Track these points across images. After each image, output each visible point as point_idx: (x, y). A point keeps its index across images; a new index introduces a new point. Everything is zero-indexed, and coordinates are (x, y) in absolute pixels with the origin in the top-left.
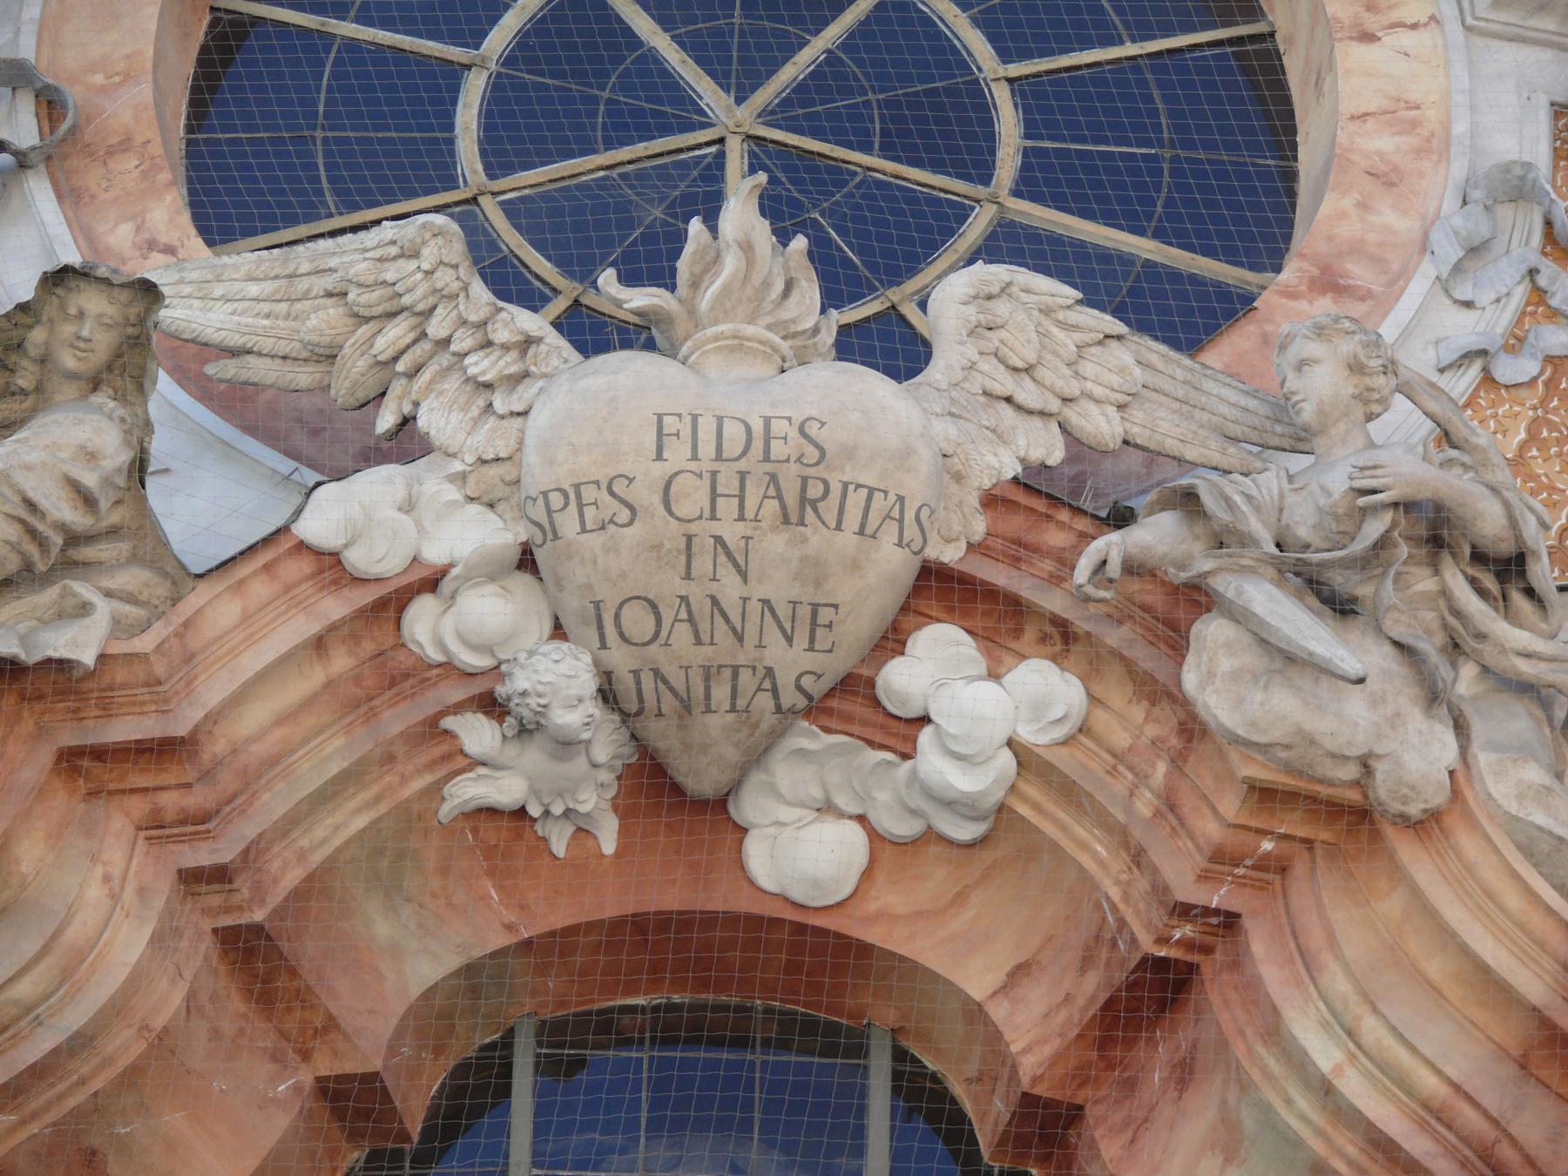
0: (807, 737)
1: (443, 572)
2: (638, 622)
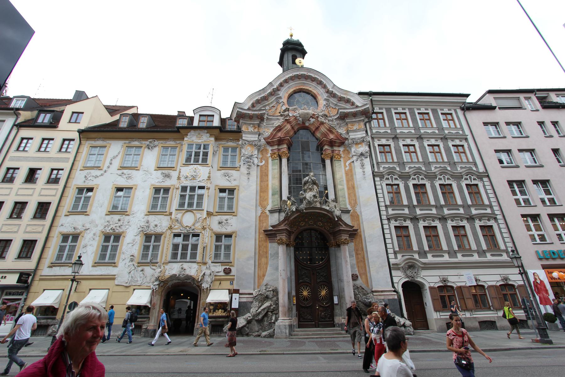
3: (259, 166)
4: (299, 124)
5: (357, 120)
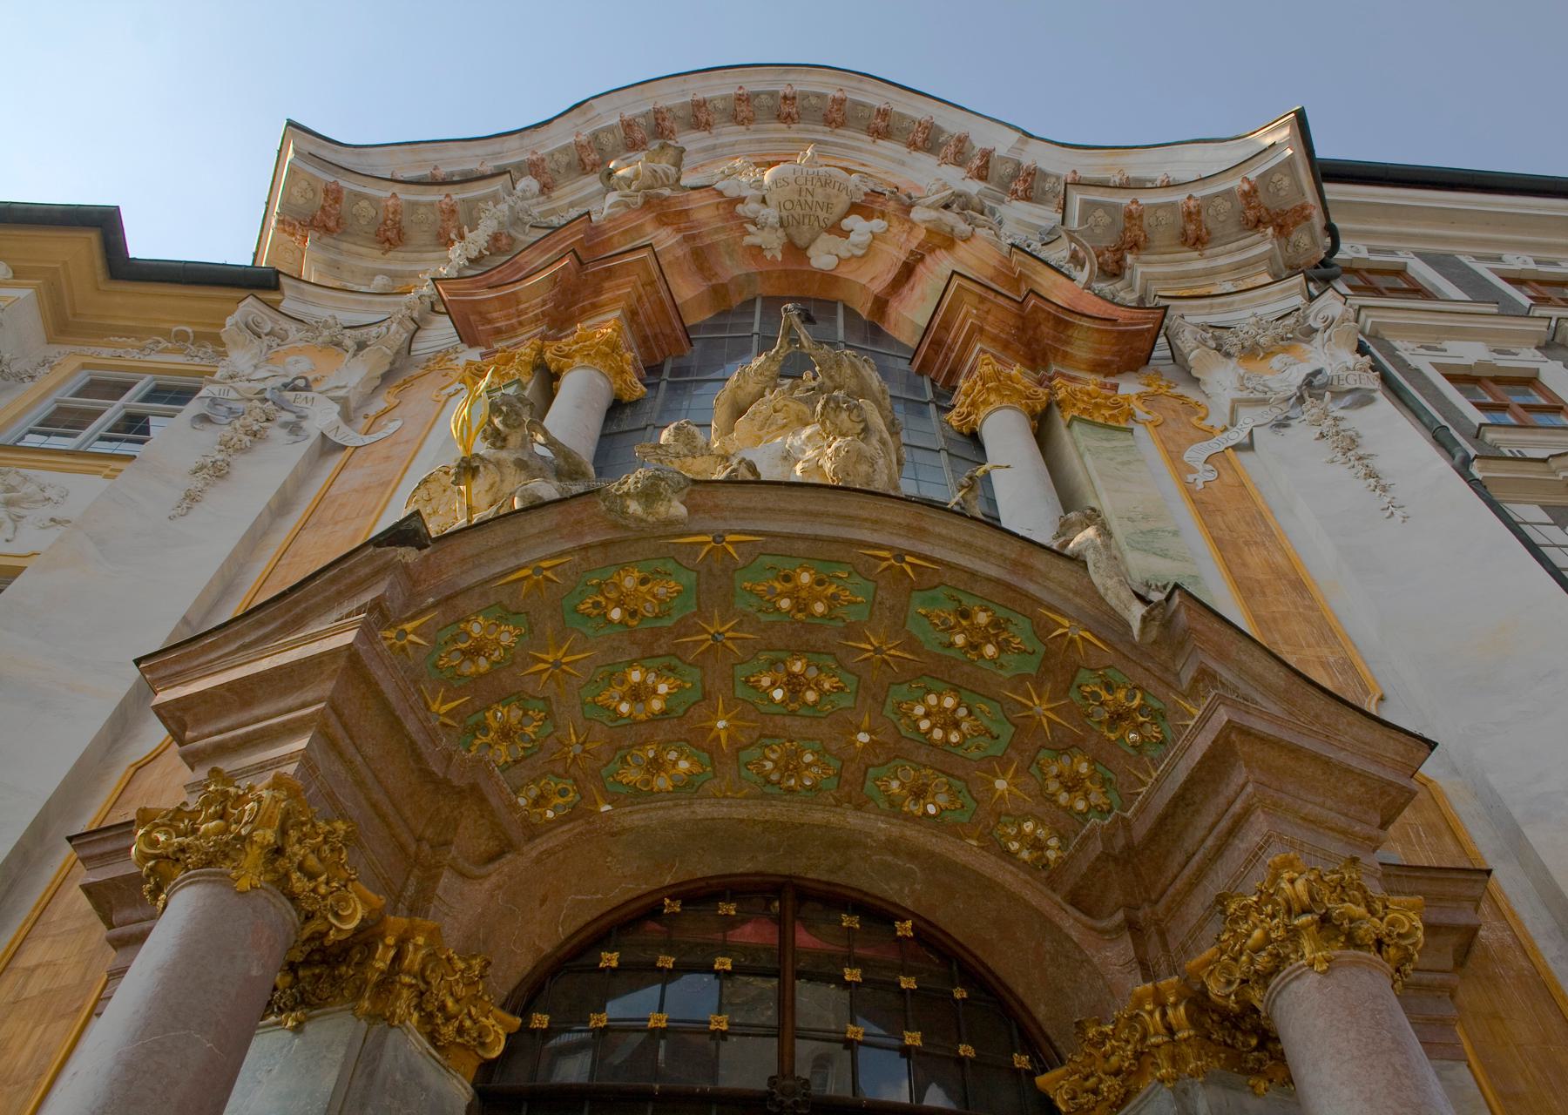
0: (825, 236)
1: (745, 198)
2: (788, 205)
3: (345, 448)
4: (758, 250)
5: (1222, 261)
